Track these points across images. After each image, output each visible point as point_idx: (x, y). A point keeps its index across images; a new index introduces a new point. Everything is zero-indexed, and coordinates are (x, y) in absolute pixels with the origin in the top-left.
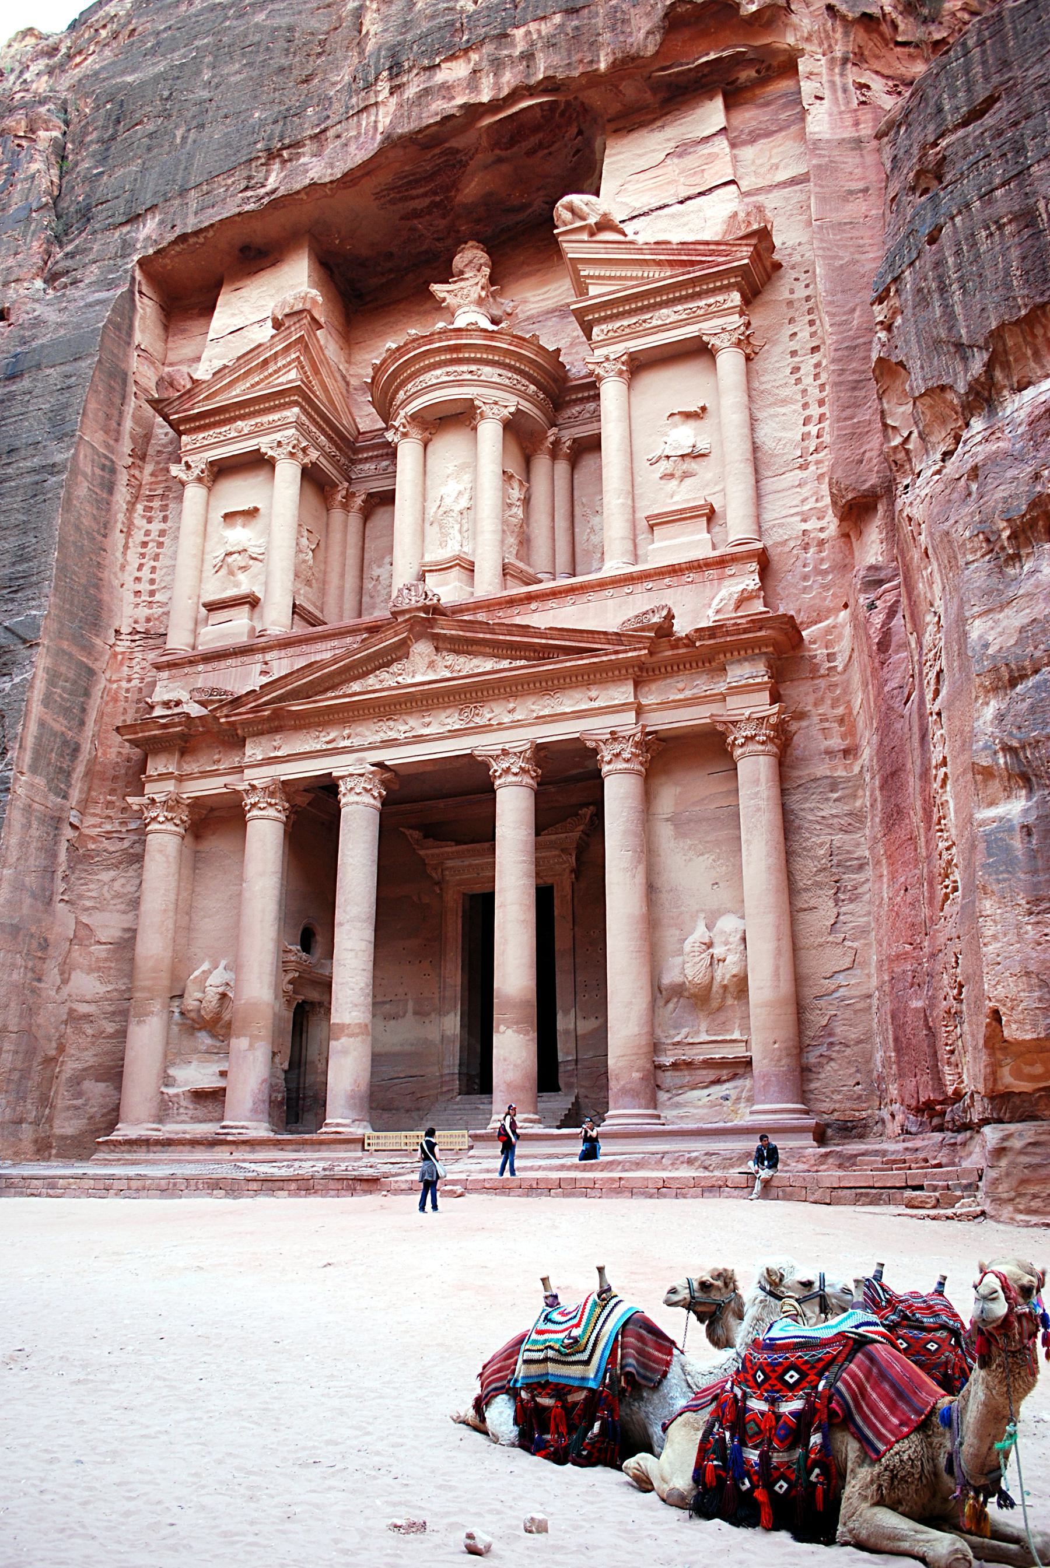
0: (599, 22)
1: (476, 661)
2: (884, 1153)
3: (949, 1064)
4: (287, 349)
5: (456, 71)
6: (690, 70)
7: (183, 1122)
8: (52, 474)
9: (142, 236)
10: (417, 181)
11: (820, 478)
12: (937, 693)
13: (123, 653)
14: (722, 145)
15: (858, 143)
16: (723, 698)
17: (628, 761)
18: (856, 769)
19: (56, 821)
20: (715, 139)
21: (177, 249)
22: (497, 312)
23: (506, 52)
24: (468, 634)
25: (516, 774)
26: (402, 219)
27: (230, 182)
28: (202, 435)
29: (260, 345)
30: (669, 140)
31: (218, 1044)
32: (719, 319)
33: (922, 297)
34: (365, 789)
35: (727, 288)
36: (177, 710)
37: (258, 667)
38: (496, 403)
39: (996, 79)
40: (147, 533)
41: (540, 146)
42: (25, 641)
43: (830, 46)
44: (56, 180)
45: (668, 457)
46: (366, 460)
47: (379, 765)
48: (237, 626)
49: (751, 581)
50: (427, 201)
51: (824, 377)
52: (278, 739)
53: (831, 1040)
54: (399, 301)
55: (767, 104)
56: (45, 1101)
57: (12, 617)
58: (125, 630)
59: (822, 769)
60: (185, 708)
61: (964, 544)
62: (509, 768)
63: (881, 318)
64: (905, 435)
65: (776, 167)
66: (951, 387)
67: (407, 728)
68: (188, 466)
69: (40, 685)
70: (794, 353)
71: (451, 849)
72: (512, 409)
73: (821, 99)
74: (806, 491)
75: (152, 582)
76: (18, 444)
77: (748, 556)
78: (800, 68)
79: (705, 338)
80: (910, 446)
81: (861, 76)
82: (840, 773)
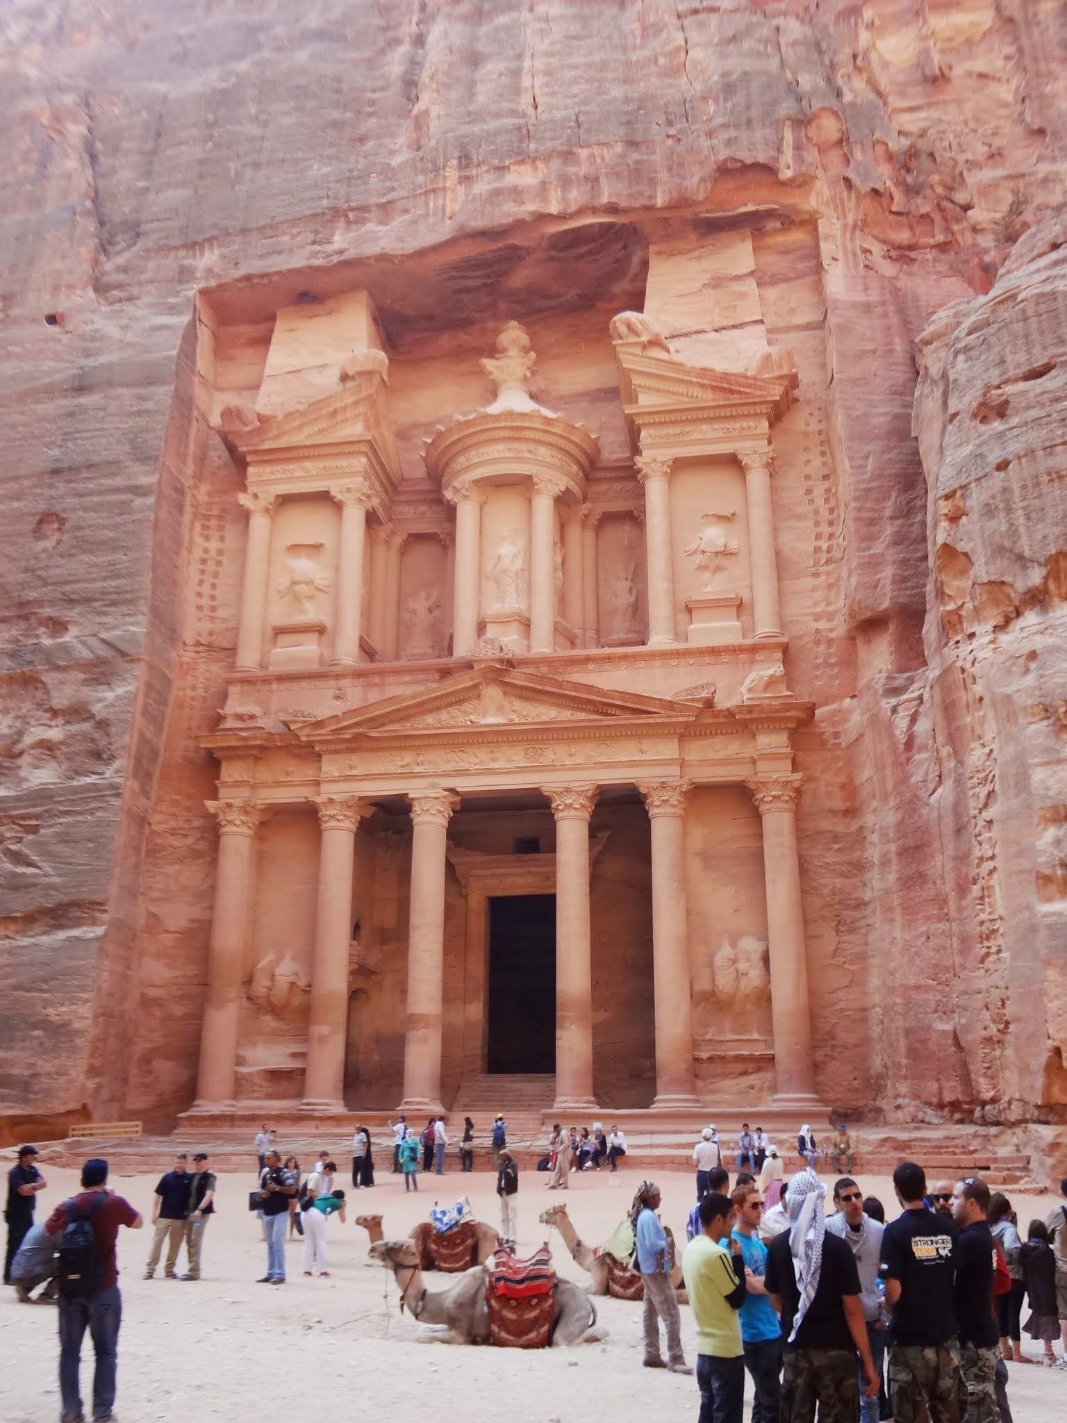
0: (658, 158)
2: (929, 1140)
3: (985, 1075)
4: (357, 403)
5: (523, 177)
8: (136, 494)
9: (201, 268)
11: (830, 586)
12: (986, 805)
13: (188, 663)
14: (751, 285)
15: (867, 308)
16: (754, 761)
18: (854, 827)
19: (141, 821)
21: (240, 285)
22: (534, 389)
23: (571, 170)
27: (295, 231)
28: (268, 469)
29: (331, 397)
30: (705, 271)
31: (284, 1027)
32: (750, 440)
33: (989, 511)
34: (440, 812)
35: (756, 415)
36: (250, 724)
37: (331, 692)
38: (550, 481)
39: (1052, 351)
40: (206, 551)
41: (590, 253)
43: (844, 212)
44: (92, 183)
45: (704, 552)
46: (406, 503)
47: (453, 791)
48: (307, 650)
49: (776, 669)
50: (477, 282)
51: (832, 503)
52: (354, 758)
53: (833, 1043)
54: (432, 359)
56: (125, 1080)
57: (108, 629)
58: (190, 641)
59: (826, 824)
60: (259, 723)
61: (1025, 708)
63: (945, 511)
64: (960, 603)
65: (792, 311)
66: (1011, 585)
67: (477, 761)
68: (256, 496)
69: (141, 697)
70: (808, 477)
71: (480, 858)
72: (563, 489)
74: (818, 595)
75: (213, 598)
76: (96, 459)
77: (776, 646)
78: (820, 229)
80: (963, 613)
81: (864, 240)
82: (840, 828)
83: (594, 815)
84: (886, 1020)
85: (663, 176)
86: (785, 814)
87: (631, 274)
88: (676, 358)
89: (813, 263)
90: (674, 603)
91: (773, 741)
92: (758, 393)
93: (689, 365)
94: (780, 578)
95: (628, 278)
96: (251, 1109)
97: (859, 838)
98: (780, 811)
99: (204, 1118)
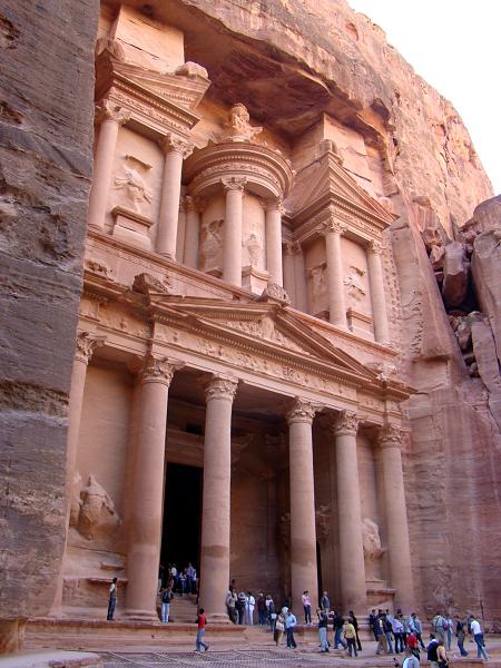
4: (191, 92)
6: (366, 125)
7: (78, 605)
10: (252, 63)
14: (364, 161)
18: (411, 464)
26: (223, 68)
28: (127, 97)
31: (86, 541)
41: (298, 97)
42: (75, 171)
47: (241, 381)
48: (142, 238)
50: (241, 71)
52: (179, 334)
60: (109, 276)
68: (117, 109)
84: (455, 575)
85: (352, 85)
91: (391, 406)
96: (77, 615)
97: (420, 471)
99: (52, 624)
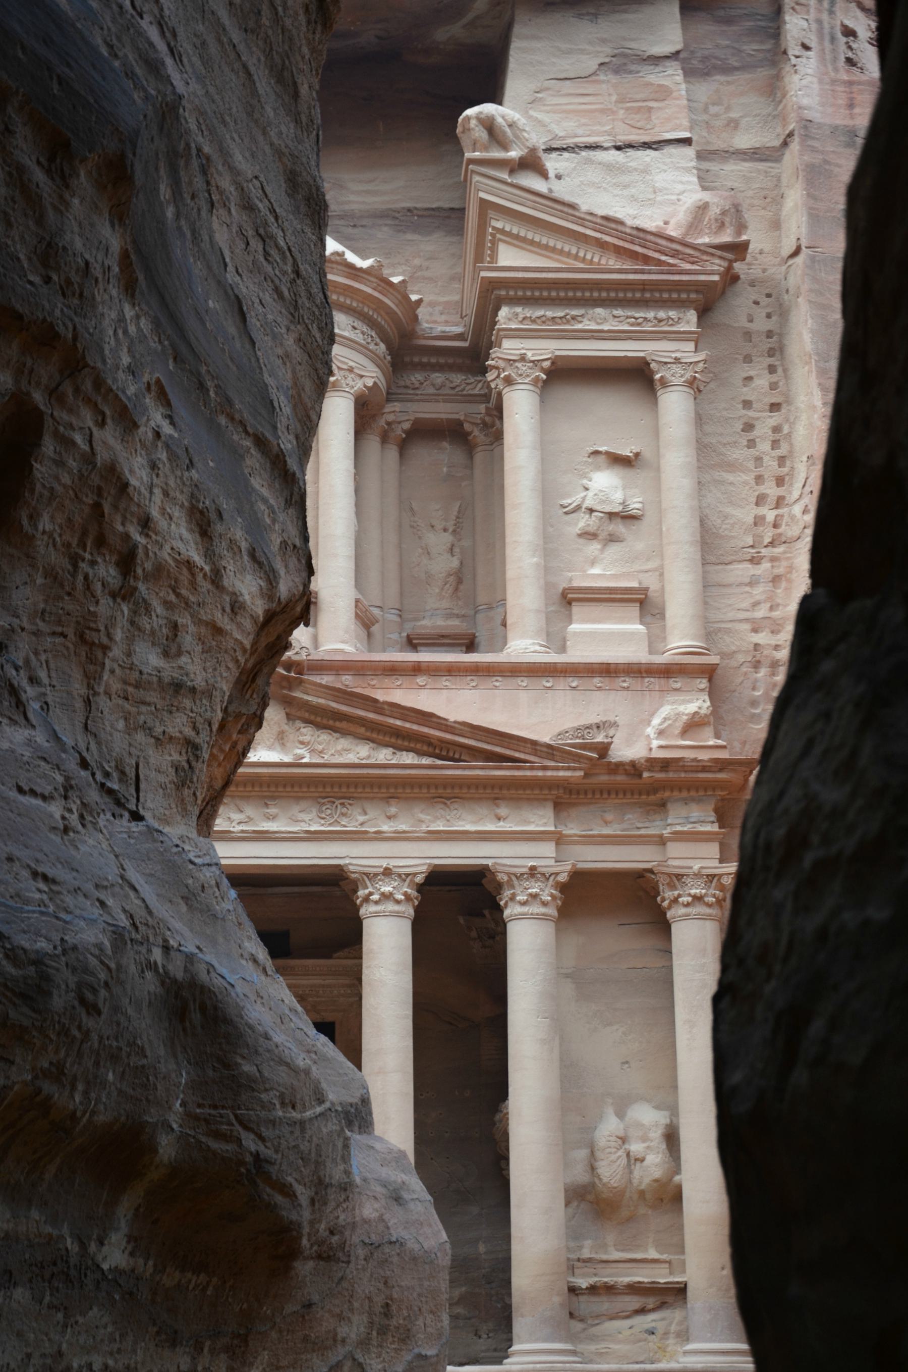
1: (344, 743)
14: (672, 77)
16: (662, 841)
17: (544, 904)
20: (668, 63)
24: (344, 708)
25: (398, 902)
38: (351, 370)
45: (591, 511)
51: (783, 450)
55: (728, 21)
62: (391, 894)
65: (733, 125)
70: (747, 404)
72: (370, 383)
73: (806, 48)
74: (758, 592)
79: (653, 365)
83: (417, 910)
86: (708, 923)
87: (470, 16)
88: (560, 190)
89: (768, 46)
90: (548, 587)
92: (688, 266)
93: (584, 208)
94: (705, 563)
95: (465, 21)
98: (702, 918)
